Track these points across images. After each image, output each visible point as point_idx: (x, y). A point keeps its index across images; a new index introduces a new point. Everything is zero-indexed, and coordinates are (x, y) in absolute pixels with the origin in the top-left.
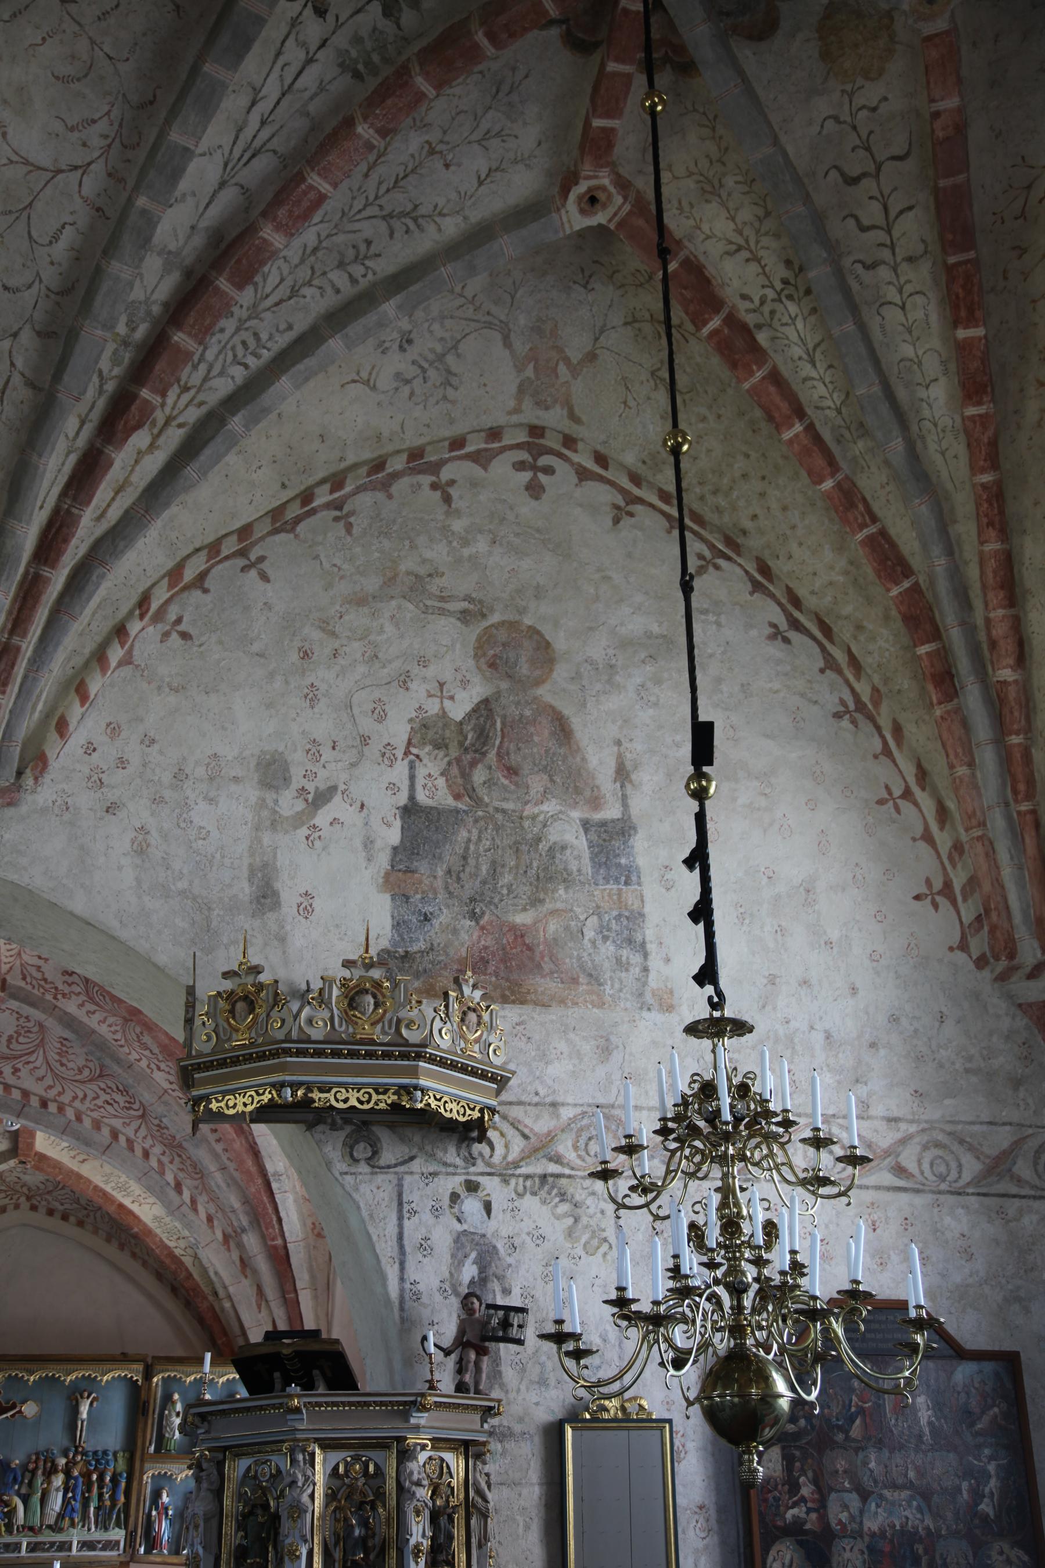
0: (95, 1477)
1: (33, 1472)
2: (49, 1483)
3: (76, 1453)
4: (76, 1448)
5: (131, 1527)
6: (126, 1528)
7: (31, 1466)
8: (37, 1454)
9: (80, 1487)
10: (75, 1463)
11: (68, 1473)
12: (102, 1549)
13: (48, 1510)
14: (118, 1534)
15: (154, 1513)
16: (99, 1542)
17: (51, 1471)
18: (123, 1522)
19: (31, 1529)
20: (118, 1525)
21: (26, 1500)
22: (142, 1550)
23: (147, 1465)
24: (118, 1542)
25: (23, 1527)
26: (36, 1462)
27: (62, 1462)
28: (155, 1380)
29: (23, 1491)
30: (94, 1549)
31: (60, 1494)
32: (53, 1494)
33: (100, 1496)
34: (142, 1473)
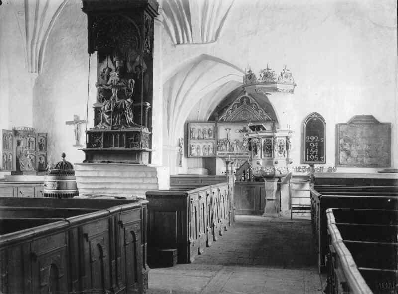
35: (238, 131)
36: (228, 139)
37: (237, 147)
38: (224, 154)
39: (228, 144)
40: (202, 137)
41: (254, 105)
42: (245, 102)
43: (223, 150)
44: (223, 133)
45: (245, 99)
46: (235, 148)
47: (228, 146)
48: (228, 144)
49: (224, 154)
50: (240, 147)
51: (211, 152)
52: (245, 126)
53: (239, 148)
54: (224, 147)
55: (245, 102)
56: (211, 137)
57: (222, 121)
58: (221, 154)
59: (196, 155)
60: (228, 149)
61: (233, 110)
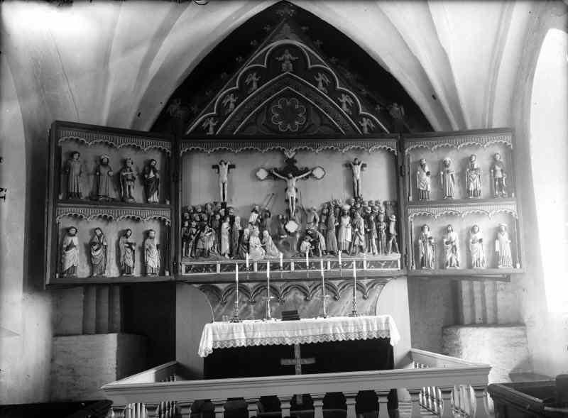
0: (372, 218)
1: (328, 215)
2: (340, 221)
3: (356, 201)
4: (355, 198)
5: (404, 253)
6: (401, 252)
7: (325, 211)
8: (329, 203)
9: (362, 227)
10: (357, 209)
11: (353, 216)
12: (384, 267)
13: (342, 240)
14: (396, 257)
15: (420, 241)
16: (382, 262)
17: (341, 214)
18: (398, 247)
19: (332, 253)
20: (394, 250)
21: (325, 234)
22: (414, 268)
23: (410, 211)
24: (396, 262)
25: (326, 251)
26: (328, 208)
27: (347, 207)
28: (407, 151)
29: (322, 228)
30: (379, 266)
31: (350, 230)
32: (343, 230)
33: (378, 230)
34: (407, 215)
35: (262, 174)
36: (224, 205)
37: (261, 236)
38: (207, 268)
39: (226, 225)
40: (113, 195)
41: (320, 78)
42: (287, 67)
43: (204, 254)
44: (200, 184)
45: (288, 56)
46: (255, 241)
47: (225, 237)
48: (226, 225)
49: (207, 268)
50: (276, 238)
51: (154, 261)
52: (290, 154)
53: (270, 241)
54: (208, 242)
55: (287, 67)
56: (155, 198)
57: (200, 135)
58: (199, 269)
59: (83, 272)
60: (226, 247)
61: (241, 94)
